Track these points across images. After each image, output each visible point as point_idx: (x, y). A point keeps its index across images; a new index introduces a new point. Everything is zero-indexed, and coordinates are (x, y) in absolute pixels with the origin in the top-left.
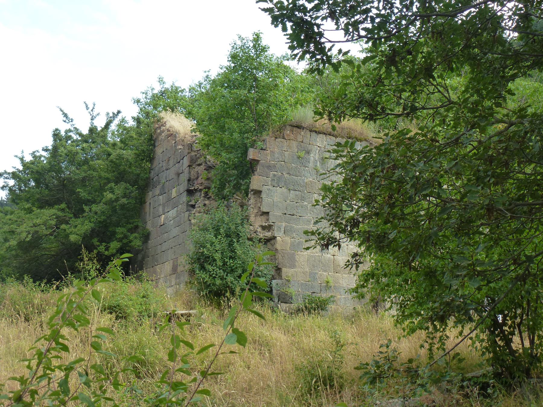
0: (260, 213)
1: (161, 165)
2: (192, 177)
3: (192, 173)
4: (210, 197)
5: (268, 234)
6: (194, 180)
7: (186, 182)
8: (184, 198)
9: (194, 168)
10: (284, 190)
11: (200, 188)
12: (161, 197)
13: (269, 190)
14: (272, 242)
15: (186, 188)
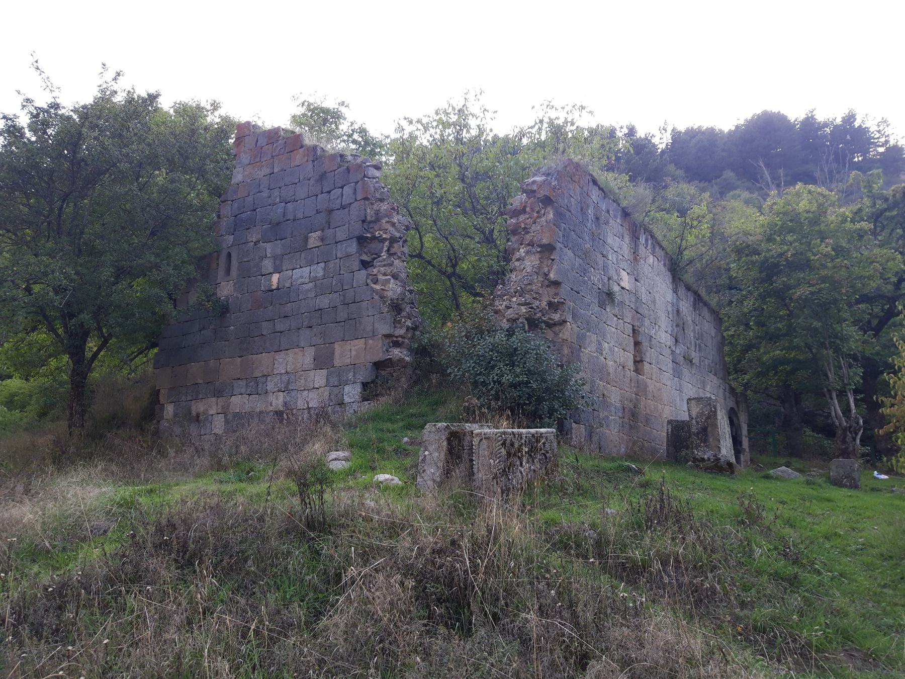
0: (547, 283)
1: (265, 194)
2: (369, 218)
3: (368, 211)
4: (395, 254)
5: (556, 317)
6: (370, 222)
7: (358, 225)
8: (353, 247)
9: (372, 204)
10: (570, 253)
11: (384, 236)
12: (268, 246)
13: (561, 248)
14: (557, 329)
15: (357, 233)
